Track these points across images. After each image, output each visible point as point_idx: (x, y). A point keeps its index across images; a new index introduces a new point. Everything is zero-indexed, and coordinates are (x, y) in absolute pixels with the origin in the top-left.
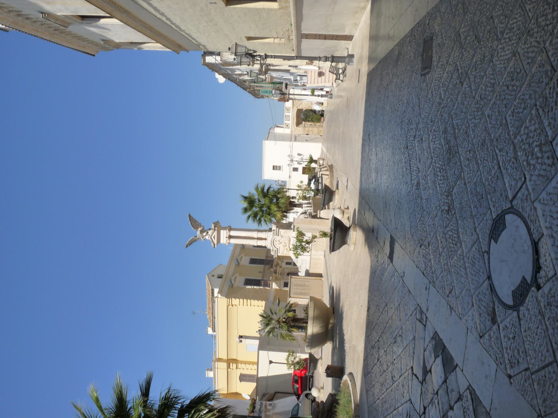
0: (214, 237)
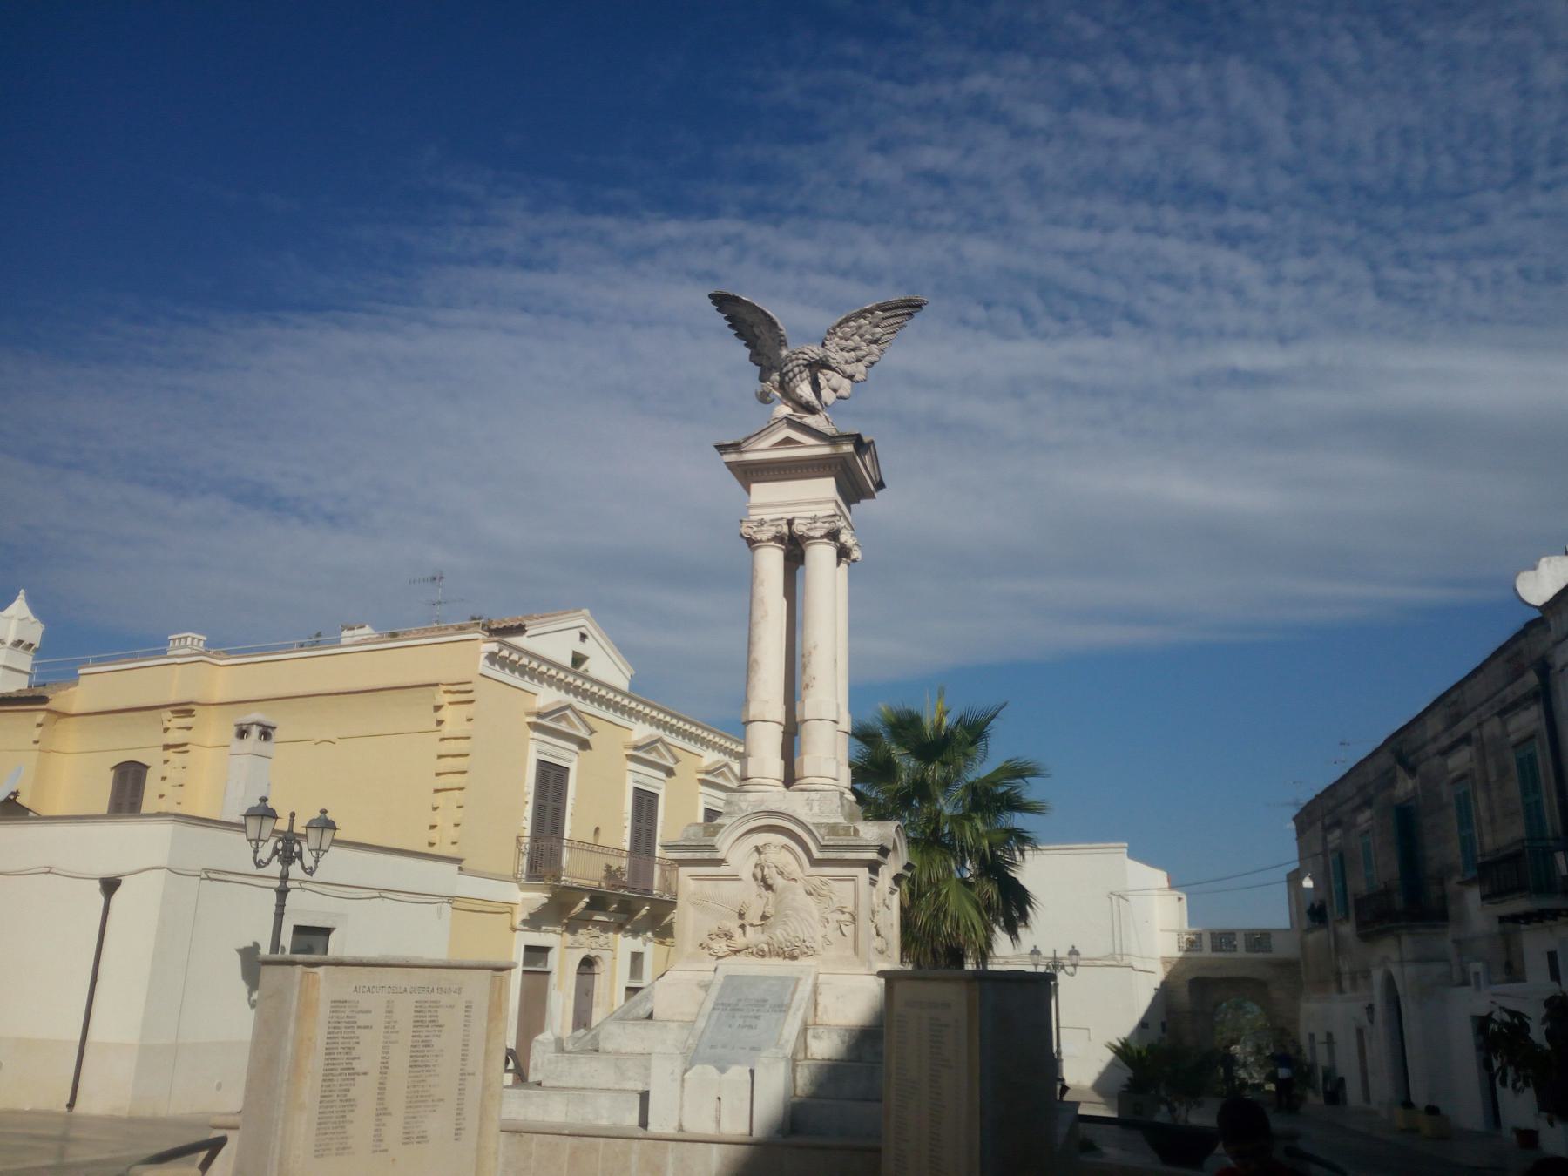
0: (787, 442)
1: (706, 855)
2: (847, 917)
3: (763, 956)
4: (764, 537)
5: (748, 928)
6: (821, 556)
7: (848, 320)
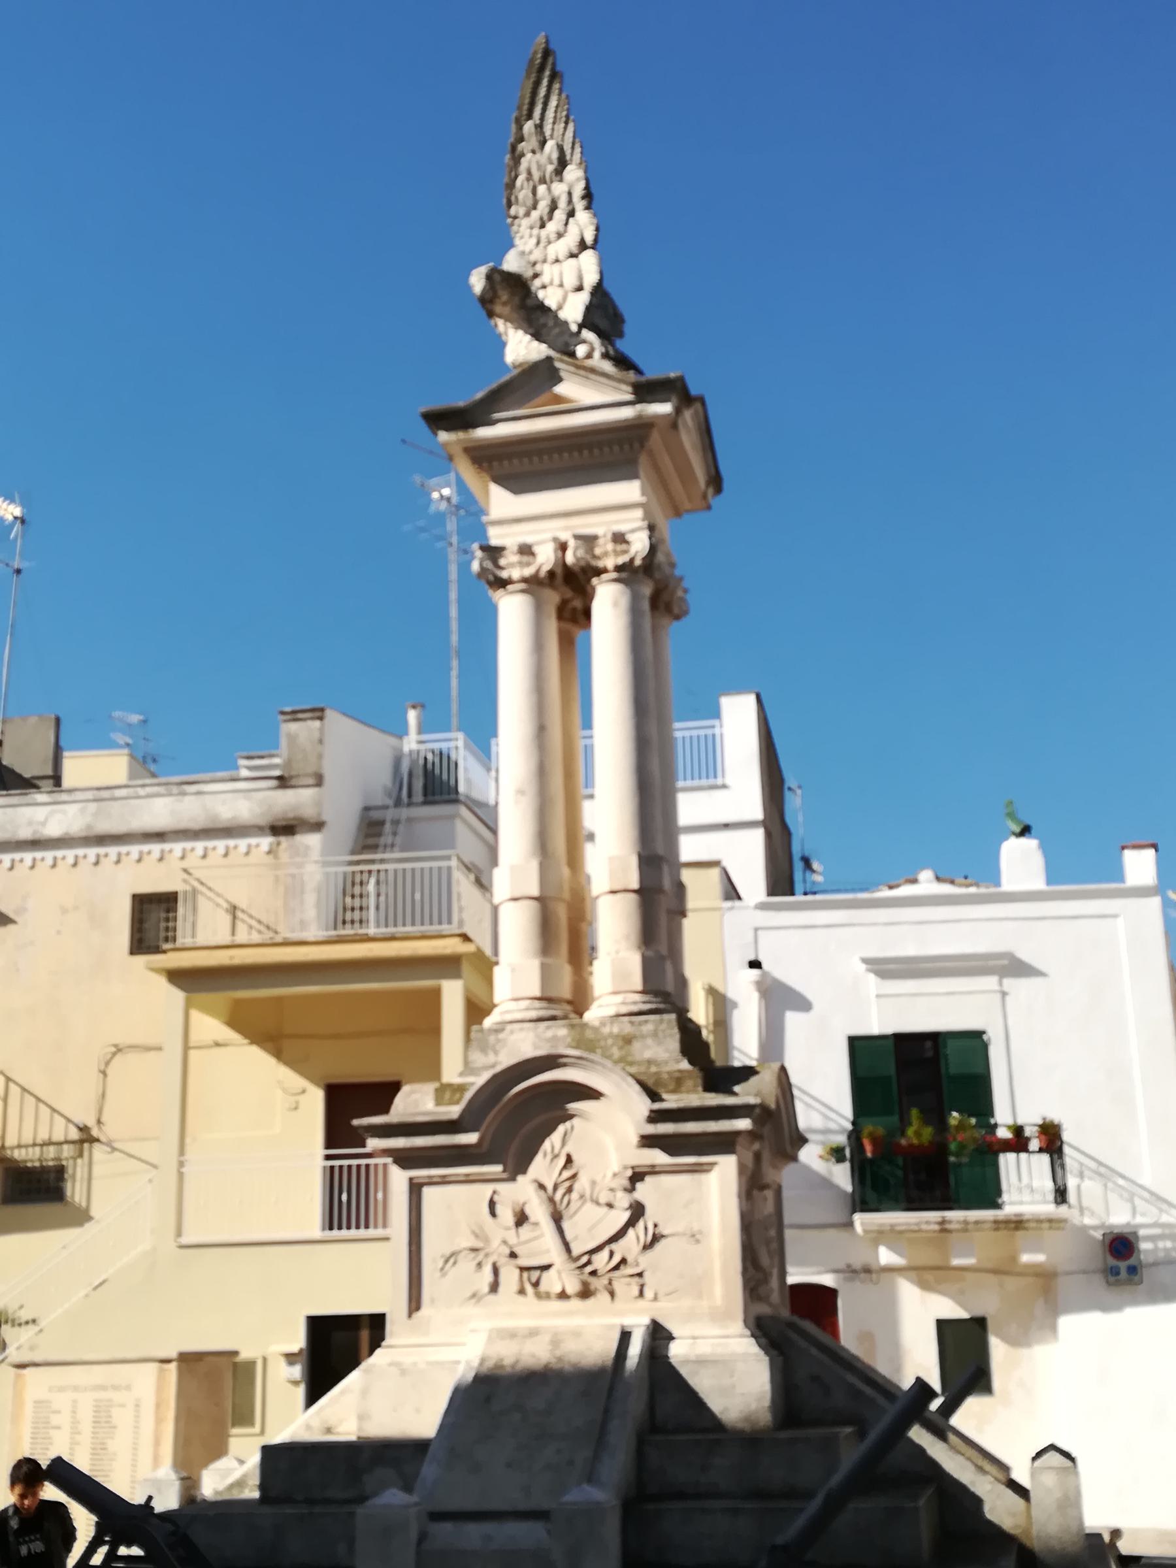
7: (511, 185)
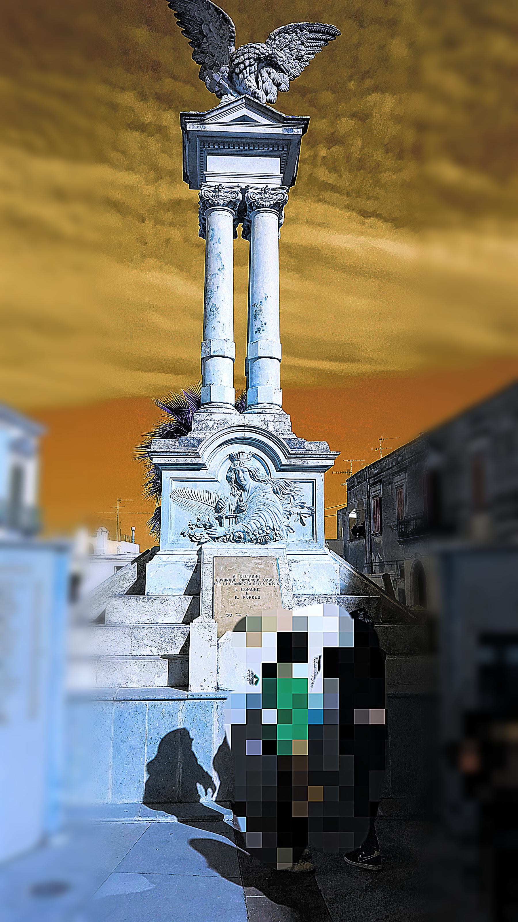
0: (244, 120)
1: (189, 461)
2: (306, 510)
3: (238, 542)
4: (221, 202)
5: (225, 521)
6: (267, 224)
